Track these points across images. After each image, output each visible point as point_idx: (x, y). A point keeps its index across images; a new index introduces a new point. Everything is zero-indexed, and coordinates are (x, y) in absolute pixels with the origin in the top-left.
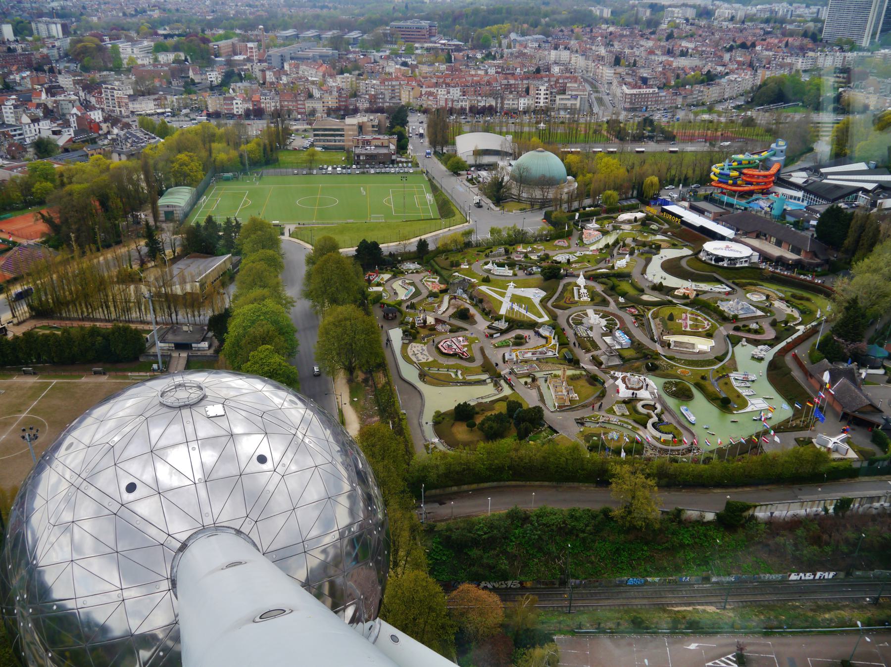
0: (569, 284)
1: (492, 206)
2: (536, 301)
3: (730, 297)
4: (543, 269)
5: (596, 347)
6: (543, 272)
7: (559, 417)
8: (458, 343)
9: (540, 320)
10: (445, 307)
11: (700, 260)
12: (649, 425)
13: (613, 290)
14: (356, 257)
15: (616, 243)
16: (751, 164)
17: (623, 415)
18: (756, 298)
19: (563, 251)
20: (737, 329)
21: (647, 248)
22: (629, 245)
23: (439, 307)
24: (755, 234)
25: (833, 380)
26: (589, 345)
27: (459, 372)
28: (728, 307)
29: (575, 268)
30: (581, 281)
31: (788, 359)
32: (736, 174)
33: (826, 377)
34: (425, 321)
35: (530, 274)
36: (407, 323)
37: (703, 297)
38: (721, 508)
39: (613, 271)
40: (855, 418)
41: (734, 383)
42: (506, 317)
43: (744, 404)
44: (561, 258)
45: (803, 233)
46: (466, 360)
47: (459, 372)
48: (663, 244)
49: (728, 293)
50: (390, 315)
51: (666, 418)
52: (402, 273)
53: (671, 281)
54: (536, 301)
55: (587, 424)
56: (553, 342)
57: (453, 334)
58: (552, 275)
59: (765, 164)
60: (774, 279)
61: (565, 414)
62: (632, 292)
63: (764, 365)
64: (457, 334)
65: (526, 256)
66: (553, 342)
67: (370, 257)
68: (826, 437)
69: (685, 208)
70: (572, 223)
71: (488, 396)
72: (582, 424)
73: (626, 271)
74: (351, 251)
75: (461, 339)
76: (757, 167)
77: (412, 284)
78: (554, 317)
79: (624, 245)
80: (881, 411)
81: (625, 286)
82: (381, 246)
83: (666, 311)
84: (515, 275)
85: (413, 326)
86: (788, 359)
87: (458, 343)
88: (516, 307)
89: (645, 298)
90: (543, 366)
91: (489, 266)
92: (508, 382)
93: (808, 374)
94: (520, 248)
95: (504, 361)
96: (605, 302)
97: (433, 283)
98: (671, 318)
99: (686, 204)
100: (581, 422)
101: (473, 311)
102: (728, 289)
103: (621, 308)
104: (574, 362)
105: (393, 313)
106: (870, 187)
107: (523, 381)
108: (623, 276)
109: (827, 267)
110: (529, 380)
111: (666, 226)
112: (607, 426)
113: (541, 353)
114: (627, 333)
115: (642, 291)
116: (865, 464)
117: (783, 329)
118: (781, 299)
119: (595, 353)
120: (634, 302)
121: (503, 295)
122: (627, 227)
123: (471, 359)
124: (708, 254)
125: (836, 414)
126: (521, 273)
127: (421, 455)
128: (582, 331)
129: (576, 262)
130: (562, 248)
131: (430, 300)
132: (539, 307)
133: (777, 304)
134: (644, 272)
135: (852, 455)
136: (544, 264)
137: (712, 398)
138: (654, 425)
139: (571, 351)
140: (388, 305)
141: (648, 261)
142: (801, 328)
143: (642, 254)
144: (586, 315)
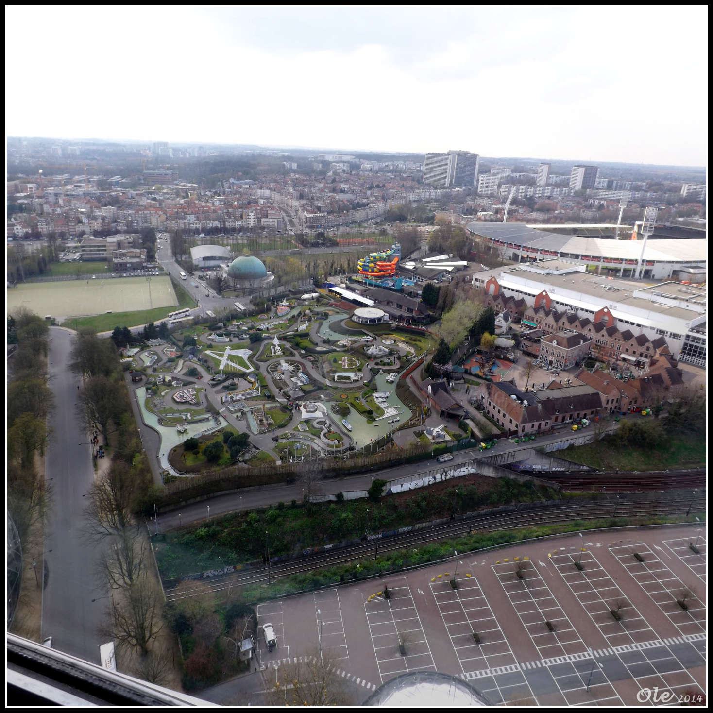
0: (268, 344)
1: (216, 294)
2: (245, 357)
3: (373, 343)
4: (250, 335)
5: (286, 385)
6: (251, 339)
7: (261, 437)
8: (188, 394)
9: (248, 371)
10: (180, 368)
11: (353, 321)
12: (322, 436)
13: (297, 346)
14: (112, 337)
15: (300, 313)
16: (381, 259)
17: (304, 431)
18: (388, 342)
19: (265, 322)
20: (377, 364)
21: (320, 316)
22: (308, 315)
23: (175, 368)
24: (386, 303)
25: (435, 391)
26: (281, 385)
27: (189, 415)
28: (372, 350)
29: (272, 333)
30: (276, 341)
31: (408, 381)
32: (372, 265)
33: (430, 389)
34: (164, 381)
35: (240, 339)
36: (150, 383)
37: (355, 345)
38: (370, 486)
39: (297, 333)
40: (448, 414)
41: (376, 400)
42: (223, 371)
43: (383, 414)
44: (262, 326)
45: (415, 299)
46: (194, 405)
47: (189, 415)
48: (330, 313)
49: (371, 341)
50: (137, 378)
51: (333, 429)
52: (148, 346)
53: (335, 336)
54: (245, 357)
55: (280, 441)
56: (257, 385)
57: (185, 387)
58: (256, 339)
59: (389, 258)
60: (399, 330)
61: (264, 435)
62: (311, 346)
63: (394, 385)
64: (188, 386)
65: (238, 328)
66: (257, 385)
67: (122, 338)
68: (431, 429)
69: (343, 288)
70: (270, 303)
71: (210, 430)
72: (277, 441)
73: (307, 331)
74: (109, 333)
75: (190, 390)
76: (385, 260)
77: (156, 353)
78: (257, 368)
79: (305, 315)
80: (463, 407)
81: (305, 342)
82: (129, 328)
83: (330, 356)
84: (231, 341)
85: (155, 384)
86: (408, 381)
87: (188, 394)
88: (230, 363)
89: (318, 349)
90: (250, 402)
91: (212, 336)
92: (224, 418)
93: (420, 389)
94: (234, 322)
95: (222, 403)
96: (292, 355)
97: (171, 351)
98: (335, 361)
99: (344, 285)
100: (276, 439)
101: (200, 369)
102: (371, 338)
103: (302, 358)
104: (271, 398)
105: (138, 376)
106: (450, 269)
107: (235, 415)
108: (305, 335)
109: (429, 319)
110: (240, 414)
111: (332, 301)
112: (294, 440)
113: (248, 394)
114: (306, 373)
115: (317, 345)
116: (456, 443)
117: (405, 362)
118: (403, 342)
119: (285, 390)
120: (310, 352)
121: (222, 355)
122: (306, 303)
123: (197, 404)
124: (359, 317)
125: (437, 412)
126: (235, 340)
127: (159, 483)
128: (277, 375)
129: (273, 329)
130: (263, 320)
131: (169, 364)
132: (247, 362)
133: (401, 345)
134: (318, 332)
135: (448, 438)
136: (251, 332)
137: (363, 412)
138: (325, 435)
139: (269, 390)
140: (136, 371)
141: (321, 324)
142: (416, 359)
143: (316, 320)
144: (280, 364)
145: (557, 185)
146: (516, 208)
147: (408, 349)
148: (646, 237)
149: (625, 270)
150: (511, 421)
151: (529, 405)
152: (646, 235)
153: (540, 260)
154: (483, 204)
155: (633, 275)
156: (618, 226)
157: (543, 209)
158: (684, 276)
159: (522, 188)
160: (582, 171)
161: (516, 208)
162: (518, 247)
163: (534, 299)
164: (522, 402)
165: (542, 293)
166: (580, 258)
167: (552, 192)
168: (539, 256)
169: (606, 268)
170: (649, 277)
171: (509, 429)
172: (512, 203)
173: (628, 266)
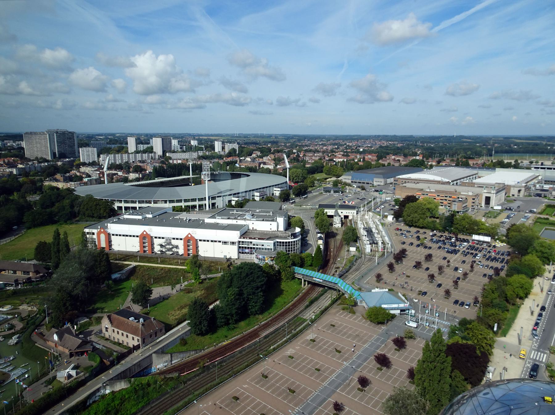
25: (60, 337)
33: (56, 337)
145: (144, 152)
146: (116, 172)
147: (30, 309)
148: (206, 182)
149: (200, 206)
150: (133, 339)
151: (144, 321)
153: (139, 208)
154: (87, 171)
155: (205, 208)
156: (191, 176)
157: (138, 169)
158: (233, 203)
159: (118, 156)
161: (116, 172)
162: (121, 201)
163: (138, 238)
164: (139, 321)
165: (143, 233)
166: (168, 202)
167: (142, 157)
168: (137, 205)
169: (188, 206)
170: (215, 208)
171: (133, 345)
173: (201, 203)
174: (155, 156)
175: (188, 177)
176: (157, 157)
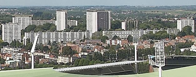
146: (42, 54)
148: (160, 68)
152: (160, 65)
156: (136, 61)
159: (45, 35)
160: (94, 15)
161: (42, 54)
172: (36, 49)
174: (88, 34)
175: (132, 62)
176: (91, 36)
